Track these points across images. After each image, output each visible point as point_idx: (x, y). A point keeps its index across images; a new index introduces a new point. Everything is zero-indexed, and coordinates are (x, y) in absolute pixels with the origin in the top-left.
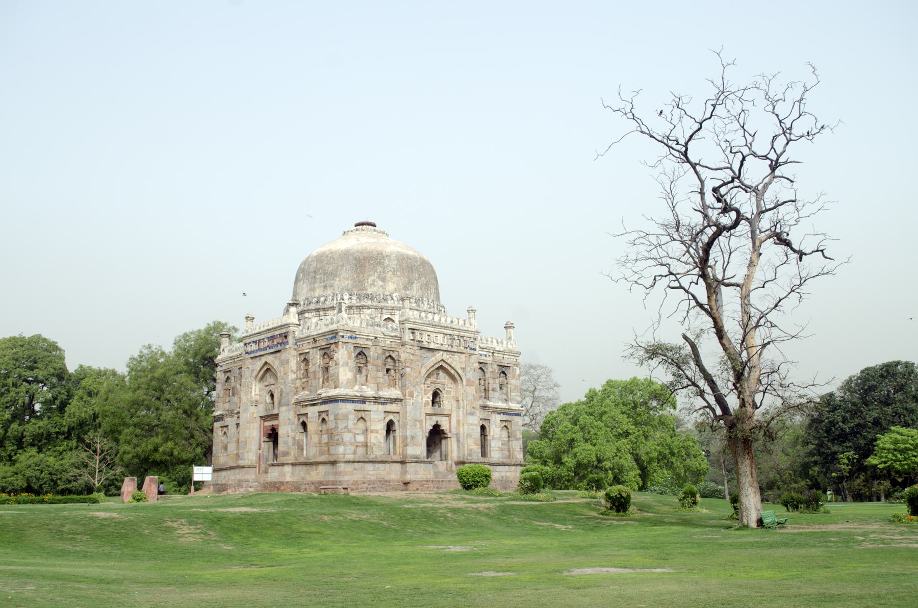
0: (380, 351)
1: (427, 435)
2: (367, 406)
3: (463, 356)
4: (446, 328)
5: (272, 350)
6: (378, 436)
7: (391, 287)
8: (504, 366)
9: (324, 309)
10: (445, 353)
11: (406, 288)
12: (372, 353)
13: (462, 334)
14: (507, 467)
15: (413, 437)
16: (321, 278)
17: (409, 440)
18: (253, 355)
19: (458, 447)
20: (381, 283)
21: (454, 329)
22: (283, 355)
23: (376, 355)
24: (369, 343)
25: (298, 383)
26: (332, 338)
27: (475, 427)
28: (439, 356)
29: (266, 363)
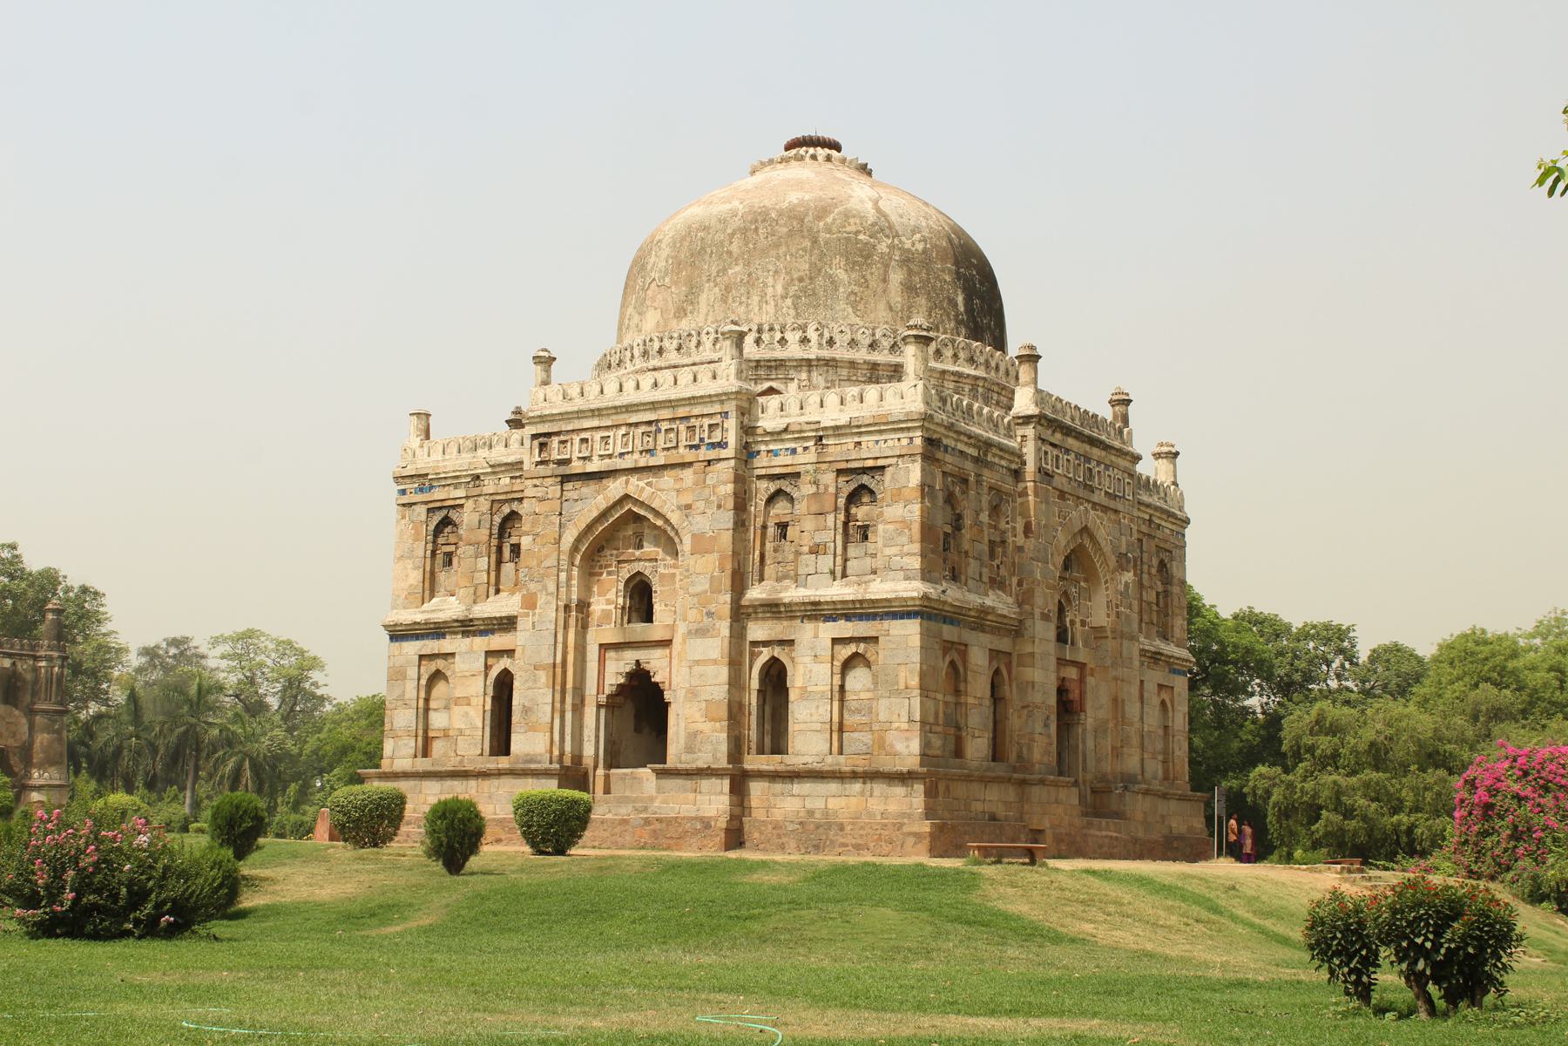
0: (484, 505)
1: (603, 699)
2: (446, 645)
3: (688, 474)
4: (630, 408)
8: (864, 471)
10: (634, 480)
11: (681, 313)
13: (681, 412)
14: (833, 787)
15: (526, 710)
17: (516, 717)
21: (654, 406)
23: (476, 517)
24: (461, 493)
27: (710, 669)
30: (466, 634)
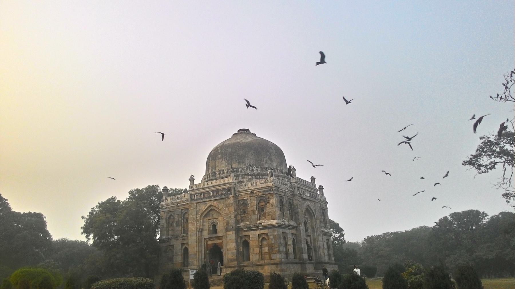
0: (287, 199)
5: (217, 198)
6: (290, 249)
7: (275, 164)
9: (242, 175)
12: (285, 200)
16: (236, 158)
18: (198, 201)
19: (316, 254)
20: (269, 162)
22: (227, 202)
24: (283, 194)
25: (239, 217)
26: (267, 191)
28: (307, 203)
29: (211, 205)
30: (289, 229)
